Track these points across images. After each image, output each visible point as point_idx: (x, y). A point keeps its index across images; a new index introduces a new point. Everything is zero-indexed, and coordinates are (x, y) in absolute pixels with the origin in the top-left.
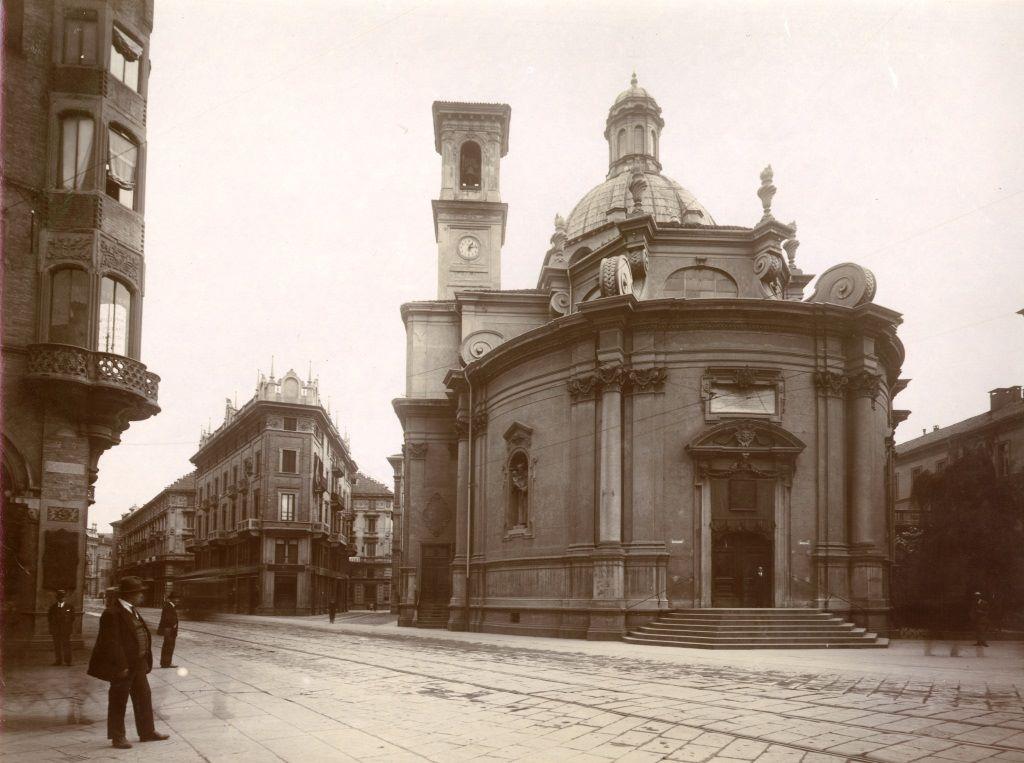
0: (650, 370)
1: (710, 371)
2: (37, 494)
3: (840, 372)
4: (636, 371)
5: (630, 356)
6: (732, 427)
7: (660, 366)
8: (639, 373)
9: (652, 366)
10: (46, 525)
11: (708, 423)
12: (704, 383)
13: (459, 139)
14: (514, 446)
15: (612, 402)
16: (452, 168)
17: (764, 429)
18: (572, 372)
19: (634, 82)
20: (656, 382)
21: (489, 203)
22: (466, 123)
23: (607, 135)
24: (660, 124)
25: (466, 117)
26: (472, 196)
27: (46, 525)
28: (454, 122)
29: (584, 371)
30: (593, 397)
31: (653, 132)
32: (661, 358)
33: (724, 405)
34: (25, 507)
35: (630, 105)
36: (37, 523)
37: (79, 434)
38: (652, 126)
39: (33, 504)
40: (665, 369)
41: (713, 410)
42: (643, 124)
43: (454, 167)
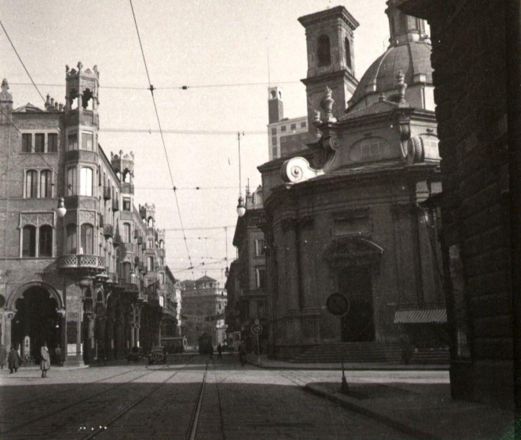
1: (334, 214)
2: (65, 308)
3: (406, 203)
5: (297, 211)
6: (340, 246)
9: (306, 214)
10: (68, 320)
13: (316, 34)
16: (313, 56)
17: (359, 243)
21: (336, 72)
22: (319, 24)
25: (319, 20)
26: (325, 70)
27: (68, 320)
28: (311, 26)
32: (311, 210)
33: (341, 233)
34: (61, 314)
36: (64, 319)
37: (76, 285)
39: (63, 312)
40: (310, 217)
43: (314, 54)
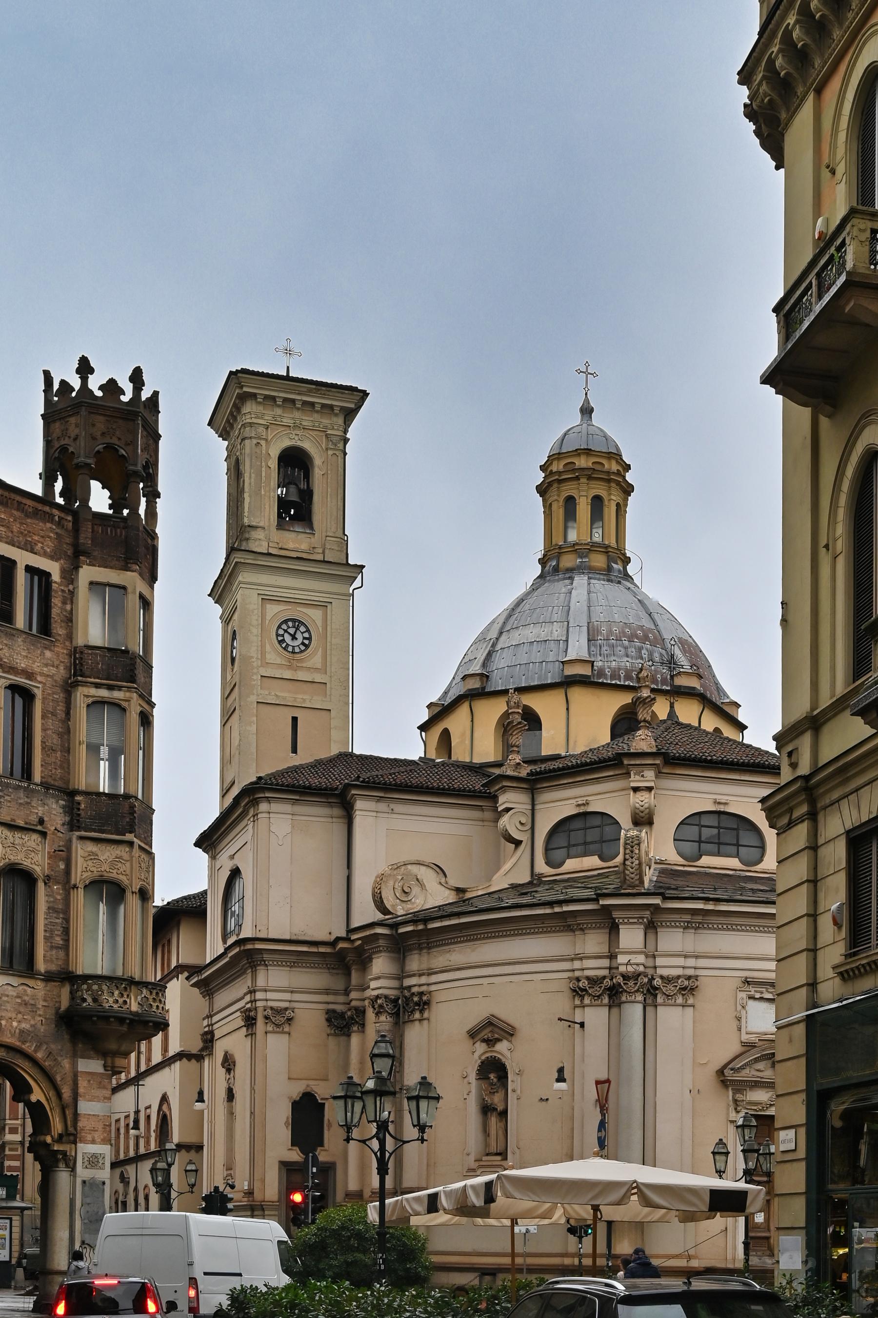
0: (679, 977)
1: (747, 982)
4: (662, 977)
5: (654, 957)
7: (690, 972)
8: (667, 980)
11: (744, 1044)
12: (743, 995)
14: (481, 1047)
15: (634, 1011)
18: (577, 964)
19: (587, 411)
20: (687, 988)
23: (542, 490)
24: (628, 490)
29: (596, 968)
30: (606, 1000)
31: (618, 505)
35: (582, 462)
38: (617, 497)
41: (750, 1029)
42: (603, 493)
